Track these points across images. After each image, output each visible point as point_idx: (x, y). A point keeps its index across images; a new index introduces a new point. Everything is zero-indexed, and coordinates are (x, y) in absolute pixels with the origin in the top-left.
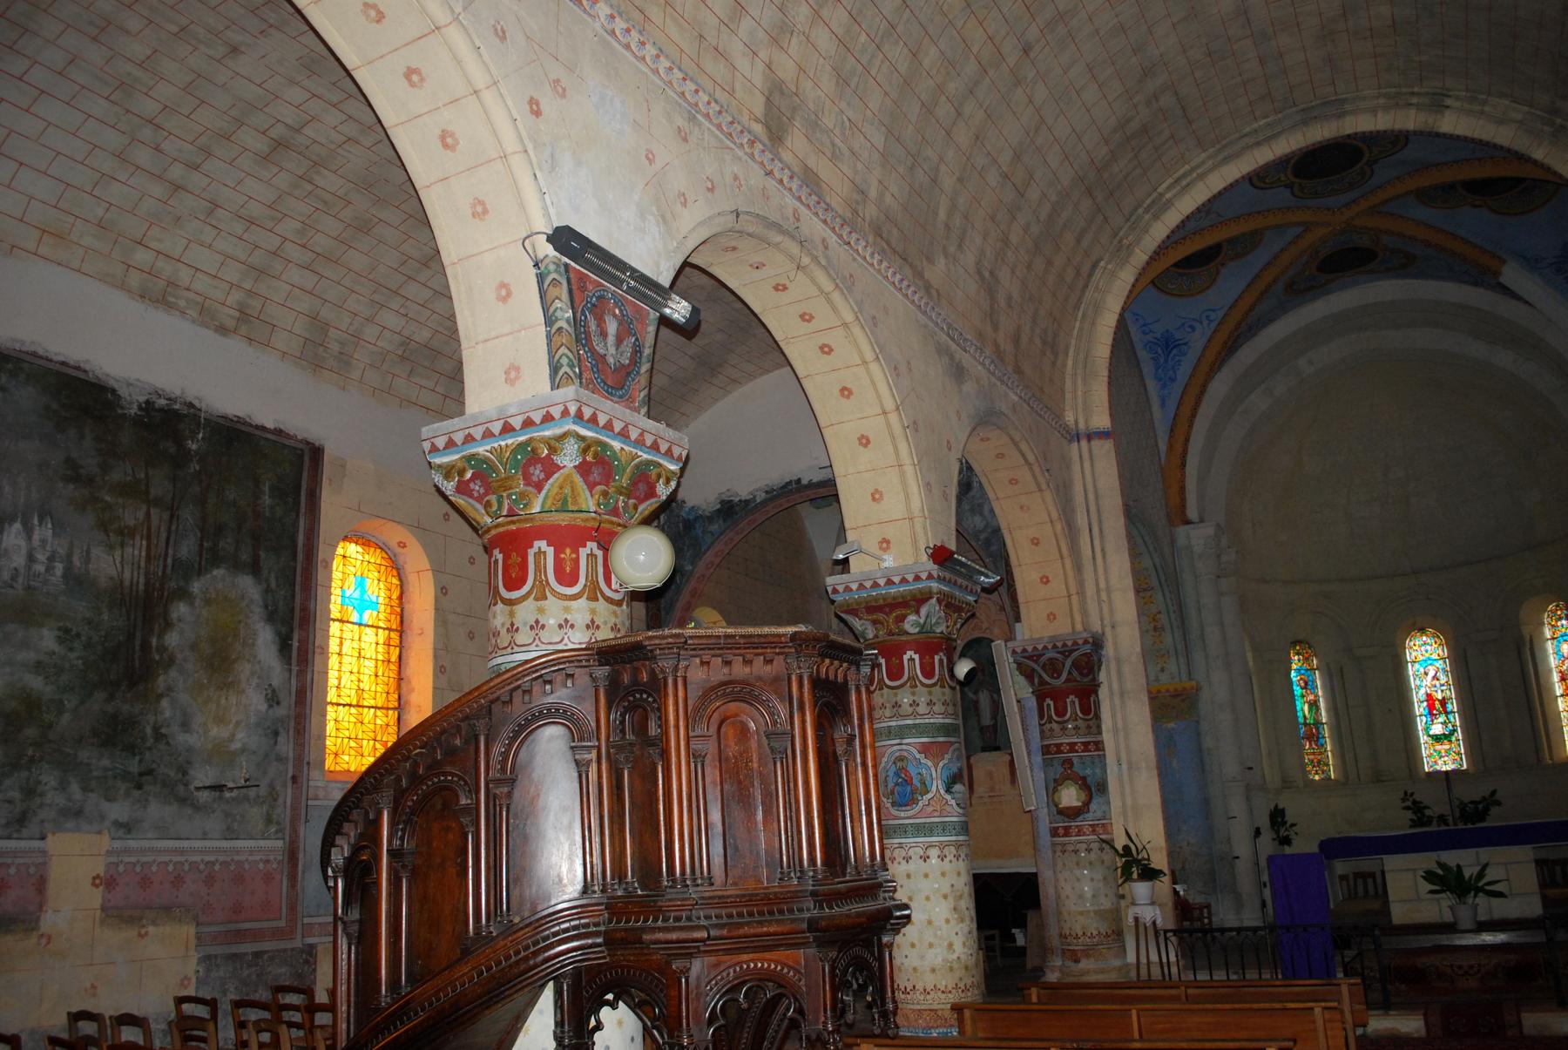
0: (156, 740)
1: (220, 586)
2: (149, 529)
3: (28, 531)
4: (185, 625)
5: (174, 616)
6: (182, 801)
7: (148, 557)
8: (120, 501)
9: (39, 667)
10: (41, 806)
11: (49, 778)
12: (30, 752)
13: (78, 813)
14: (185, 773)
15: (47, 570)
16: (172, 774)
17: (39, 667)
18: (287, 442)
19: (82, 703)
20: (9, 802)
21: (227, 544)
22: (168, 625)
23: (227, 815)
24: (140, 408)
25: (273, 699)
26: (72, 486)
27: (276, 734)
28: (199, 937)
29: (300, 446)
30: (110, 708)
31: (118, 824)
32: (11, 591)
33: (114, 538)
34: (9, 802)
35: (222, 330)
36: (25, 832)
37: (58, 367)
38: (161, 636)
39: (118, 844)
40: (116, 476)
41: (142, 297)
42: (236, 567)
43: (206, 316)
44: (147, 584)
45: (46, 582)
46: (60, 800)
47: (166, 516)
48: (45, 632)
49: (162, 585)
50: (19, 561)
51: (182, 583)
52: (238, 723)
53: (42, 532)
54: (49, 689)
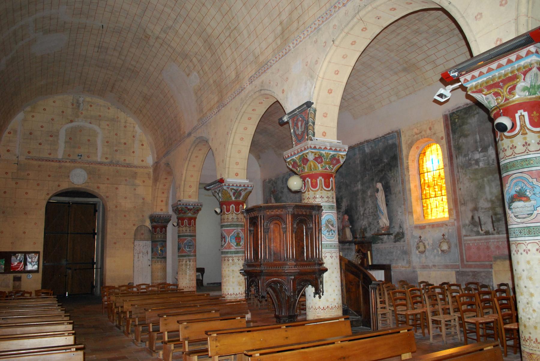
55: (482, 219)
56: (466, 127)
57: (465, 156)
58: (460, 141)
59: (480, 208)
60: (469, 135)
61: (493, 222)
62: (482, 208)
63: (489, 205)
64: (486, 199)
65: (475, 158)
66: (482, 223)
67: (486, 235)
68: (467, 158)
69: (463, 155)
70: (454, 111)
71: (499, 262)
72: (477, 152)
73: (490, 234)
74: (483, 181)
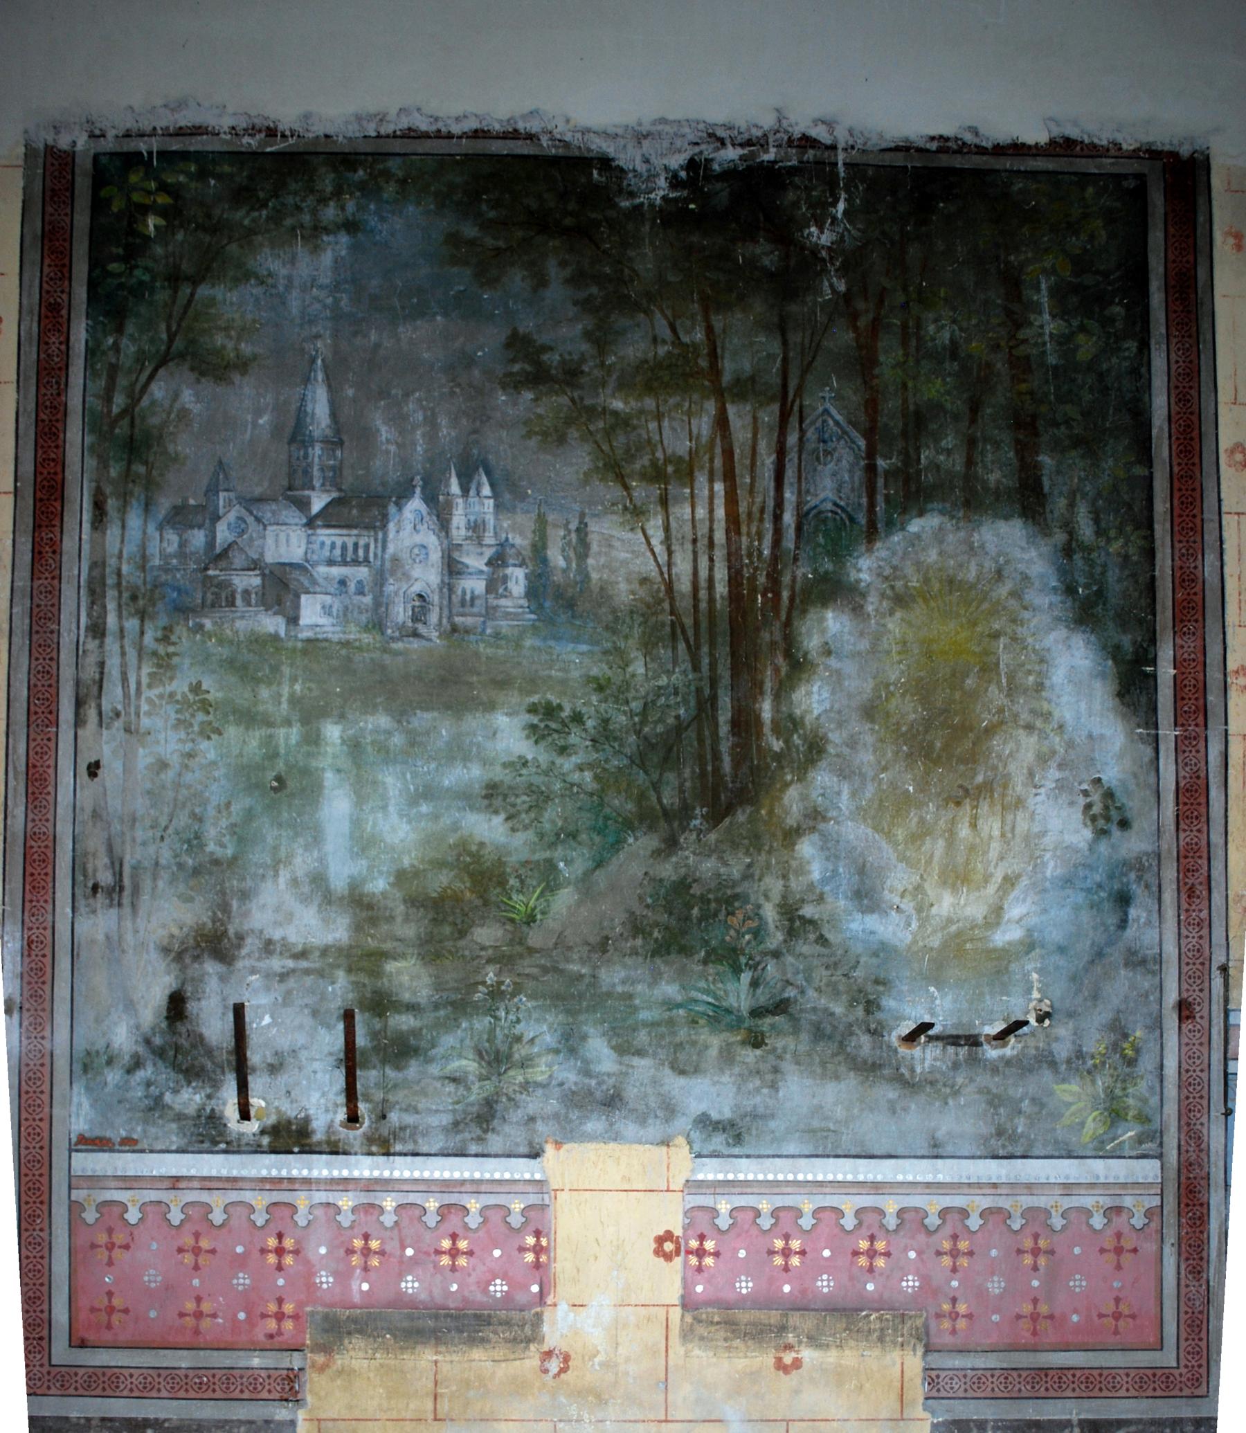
0: (791, 933)
1: (932, 556)
2: (728, 454)
3: (441, 515)
4: (843, 667)
5: (811, 643)
6: (869, 1069)
7: (733, 521)
8: (649, 403)
10: (526, 1086)
11: (538, 1028)
12: (491, 977)
13: (612, 1102)
14: (871, 1006)
15: (491, 588)
16: (838, 1009)
18: (1091, 167)
21: (942, 453)
22: (798, 667)
23: (994, 1101)
25: (1108, 814)
26: (528, 395)
27: (1123, 900)
28: (932, 1377)
29: (1134, 167)
30: (667, 870)
31: (706, 1124)
32: (415, 644)
33: (641, 491)
34: (454, 1080)
36: (495, 1142)
37: (466, 146)
38: (783, 690)
39: (711, 1171)
40: (634, 348)
42: (972, 501)
44: (734, 579)
45: (490, 612)
46: (569, 1075)
47: (769, 415)
48: (501, 720)
50: (427, 577)
51: (828, 566)
52: (1010, 882)
53: (474, 507)
54: (520, 839)
55: (260, 1023)
56: (229, 301)
57: (180, 517)
58: (158, 390)
59: (251, 944)
60: (243, 365)
61: (351, 1061)
62: (268, 947)
63: (338, 931)
64: (318, 880)
65: (269, 558)
66: (255, 1057)
67: (274, 1151)
68: (198, 538)
69: (164, 504)
70: (143, 146)
71: (356, 1356)
72: (293, 516)
73: (308, 1149)
74: (313, 739)
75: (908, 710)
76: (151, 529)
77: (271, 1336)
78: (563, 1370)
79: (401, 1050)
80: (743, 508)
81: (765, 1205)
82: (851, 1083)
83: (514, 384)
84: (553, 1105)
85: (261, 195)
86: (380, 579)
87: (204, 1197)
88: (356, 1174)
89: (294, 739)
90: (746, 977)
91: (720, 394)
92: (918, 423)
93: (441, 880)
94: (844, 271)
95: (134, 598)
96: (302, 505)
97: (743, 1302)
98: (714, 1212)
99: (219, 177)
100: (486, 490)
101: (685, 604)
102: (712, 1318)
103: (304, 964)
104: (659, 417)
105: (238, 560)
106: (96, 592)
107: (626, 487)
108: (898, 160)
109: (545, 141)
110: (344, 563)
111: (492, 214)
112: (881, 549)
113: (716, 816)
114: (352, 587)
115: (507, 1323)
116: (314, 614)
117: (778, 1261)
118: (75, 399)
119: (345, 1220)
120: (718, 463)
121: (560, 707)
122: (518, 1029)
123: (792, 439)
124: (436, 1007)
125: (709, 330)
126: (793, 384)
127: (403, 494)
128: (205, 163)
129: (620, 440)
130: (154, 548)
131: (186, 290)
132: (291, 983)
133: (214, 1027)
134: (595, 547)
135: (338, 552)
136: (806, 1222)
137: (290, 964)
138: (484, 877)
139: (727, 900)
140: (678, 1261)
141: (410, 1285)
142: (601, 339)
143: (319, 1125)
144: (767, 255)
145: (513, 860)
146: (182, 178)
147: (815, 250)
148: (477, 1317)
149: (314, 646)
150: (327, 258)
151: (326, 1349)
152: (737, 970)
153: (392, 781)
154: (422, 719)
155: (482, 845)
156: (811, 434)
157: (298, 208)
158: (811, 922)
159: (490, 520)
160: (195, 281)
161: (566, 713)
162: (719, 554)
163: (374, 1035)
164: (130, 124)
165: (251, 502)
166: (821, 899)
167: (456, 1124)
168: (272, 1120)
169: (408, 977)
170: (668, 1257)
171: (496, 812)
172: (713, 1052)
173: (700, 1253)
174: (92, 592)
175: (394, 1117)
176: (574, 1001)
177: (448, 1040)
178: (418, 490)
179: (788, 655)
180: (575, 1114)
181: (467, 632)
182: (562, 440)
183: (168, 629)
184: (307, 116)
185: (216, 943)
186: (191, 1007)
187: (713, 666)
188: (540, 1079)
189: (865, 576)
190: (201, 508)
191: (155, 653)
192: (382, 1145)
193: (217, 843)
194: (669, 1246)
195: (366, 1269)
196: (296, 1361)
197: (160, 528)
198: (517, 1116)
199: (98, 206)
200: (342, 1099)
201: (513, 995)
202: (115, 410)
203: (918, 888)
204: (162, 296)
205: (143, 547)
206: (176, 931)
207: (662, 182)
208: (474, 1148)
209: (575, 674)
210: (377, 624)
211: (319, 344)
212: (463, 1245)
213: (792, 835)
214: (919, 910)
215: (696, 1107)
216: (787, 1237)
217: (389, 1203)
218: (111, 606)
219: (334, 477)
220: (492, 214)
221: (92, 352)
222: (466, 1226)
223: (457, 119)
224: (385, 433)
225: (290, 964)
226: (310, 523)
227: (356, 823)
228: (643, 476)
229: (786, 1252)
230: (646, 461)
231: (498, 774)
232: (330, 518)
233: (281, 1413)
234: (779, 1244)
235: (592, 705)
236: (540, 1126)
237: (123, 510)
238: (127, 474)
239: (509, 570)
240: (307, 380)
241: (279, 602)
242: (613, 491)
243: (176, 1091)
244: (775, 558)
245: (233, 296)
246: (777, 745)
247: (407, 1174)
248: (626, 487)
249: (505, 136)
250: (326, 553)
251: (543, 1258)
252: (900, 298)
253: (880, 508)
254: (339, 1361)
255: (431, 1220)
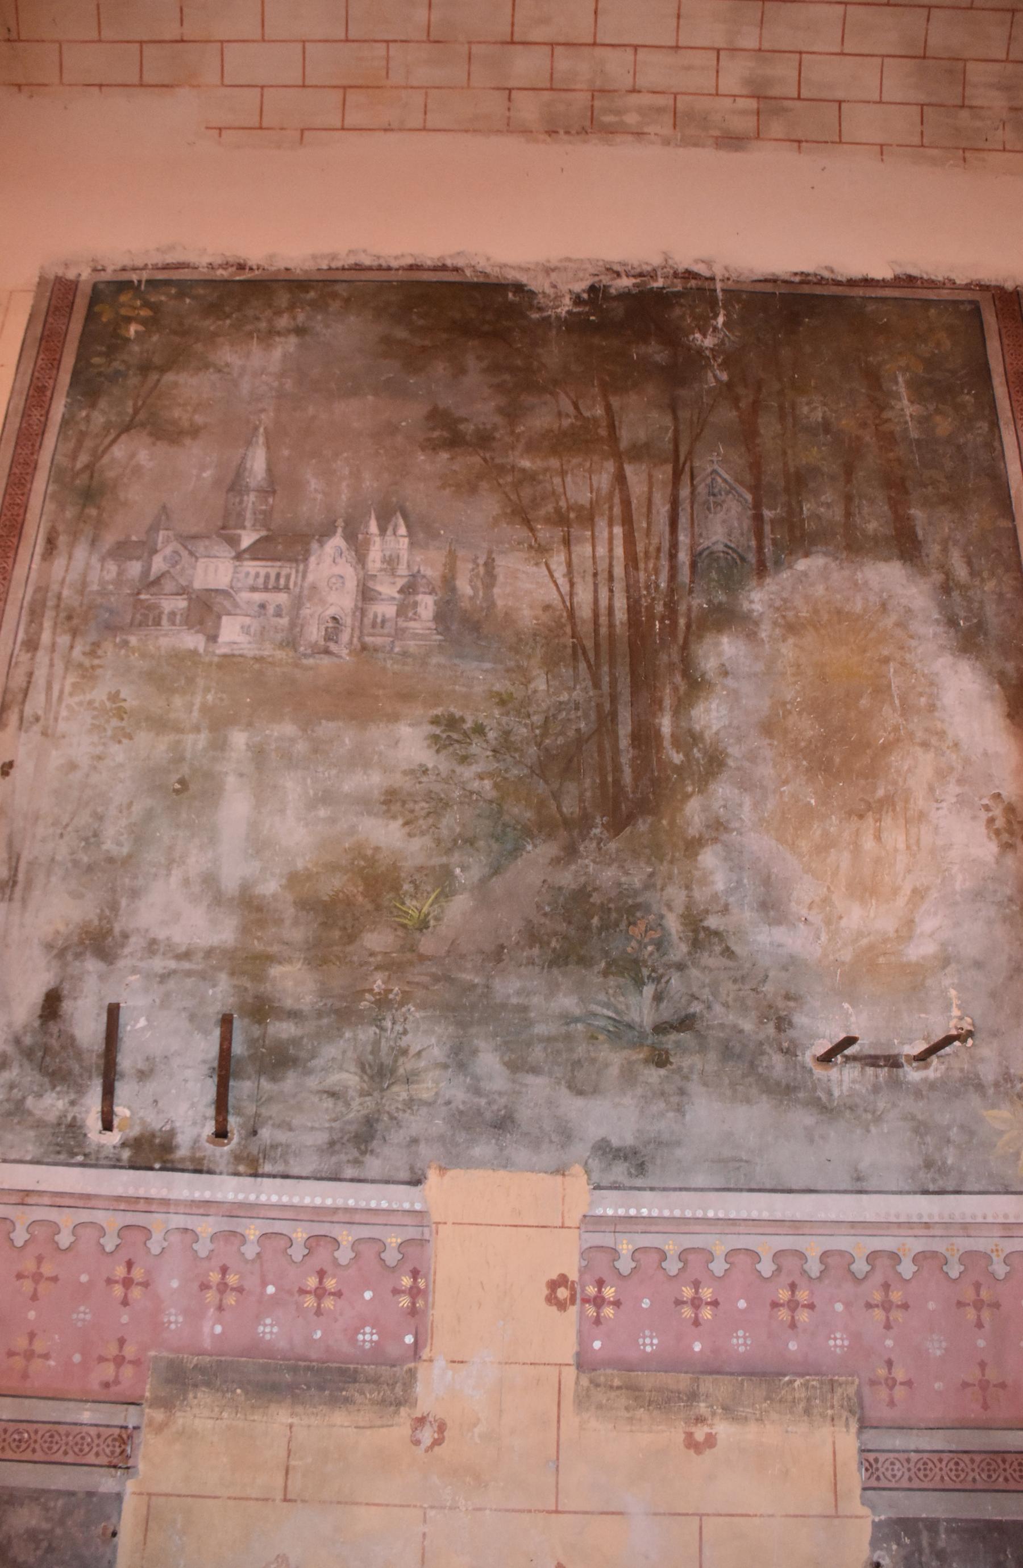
0: (696, 945)
1: (820, 590)
2: (626, 503)
3: (359, 550)
4: (737, 687)
6: (784, 1092)
7: (632, 560)
8: (554, 463)
9: (391, 801)
10: (410, 1103)
11: (425, 1040)
12: (378, 983)
13: (503, 1123)
14: (783, 1023)
16: (747, 1026)
17: (391, 801)
18: (932, 295)
19: (496, 870)
20: (333, 1094)
21: (822, 505)
22: (696, 685)
23: (921, 1128)
24: (577, 300)
26: (445, 455)
28: (869, 1461)
29: (968, 296)
30: (567, 878)
31: (607, 1151)
32: (326, 661)
33: (544, 532)
34: (333, 1094)
35: (732, 141)
36: (374, 1166)
37: (402, 276)
38: (683, 706)
41: (552, 132)
42: (854, 546)
43: (687, 124)
44: (633, 609)
45: (399, 633)
47: (664, 473)
48: (404, 730)
49: (671, 608)
50: (341, 602)
51: (721, 597)
52: (918, 894)
53: (390, 545)
54: (417, 844)
57: (122, 551)
58: (119, 451)
59: (135, 943)
60: (195, 432)
61: (225, 1070)
62: (152, 947)
63: (224, 932)
64: (210, 880)
65: (197, 585)
66: (126, 1062)
67: (133, 1167)
68: (135, 568)
69: (109, 539)
70: (135, 277)
71: (202, 1415)
73: (169, 1167)
74: (219, 745)
75: (806, 728)
76: (95, 561)
77: (107, 1385)
78: (437, 1442)
79: (278, 1060)
80: (640, 548)
81: (671, 1246)
82: (763, 1107)
83: (433, 446)
84: (439, 1125)
85: (227, 309)
86: (298, 603)
87: (53, 1215)
88: (219, 1197)
89: (200, 746)
90: (649, 990)
91: (618, 456)
92: (799, 482)
93: (336, 883)
94: (725, 365)
95: (69, 618)
96: (233, 541)
97: (645, 1364)
98: (614, 1253)
99: (193, 297)
100: (402, 530)
101: (586, 630)
102: (615, 1381)
103: (186, 965)
104: (563, 473)
105: (169, 586)
106: (35, 613)
107: (532, 530)
108: (769, 288)
109: (468, 272)
110: (266, 589)
111: (421, 322)
112: (771, 584)
113: (617, 825)
114: (271, 610)
115: (375, 1381)
116: (233, 633)
117: (687, 1312)
118: (45, 458)
119: (203, 1248)
120: (617, 510)
121: (463, 720)
122: (403, 1042)
123: (685, 492)
124: (320, 1014)
125: (608, 408)
126: (683, 450)
127: (326, 532)
128: (184, 288)
129: (527, 492)
130: (94, 577)
131: (154, 376)
132: (171, 984)
133: (86, 1027)
134: (501, 578)
135: (261, 580)
136: (718, 1267)
137: (173, 964)
138: (379, 881)
139: (627, 910)
140: (573, 1310)
141: (269, 1330)
142: (512, 414)
143: (184, 1141)
144: (657, 353)
145: (408, 865)
146: (163, 298)
147: (700, 351)
148: (342, 1372)
149: (230, 662)
150: (277, 353)
151: (166, 1404)
152: (639, 983)
153: (293, 786)
154: (326, 728)
155: (377, 849)
156: (701, 489)
157: (258, 319)
158: (716, 933)
159: (404, 555)
160: (163, 370)
161: (468, 725)
162: (619, 586)
163: (252, 1043)
164: (127, 261)
165: (188, 539)
166: (725, 910)
167: (332, 1144)
168: (135, 1132)
169: (293, 982)
170: (562, 1306)
171: (394, 817)
172: (614, 1071)
173: (599, 1302)
174: (32, 612)
175: (266, 1133)
176: (466, 1011)
177: (330, 1051)
178: (340, 530)
179: (686, 674)
180: (461, 1137)
181: (376, 650)
182: (473, 489)
183: (96, 645)
184: (272, 256)
185: (99, 942)
186: (67, 1006)
187: (613, 683)
188: (425, 1096)
189: (758, 607)
190: (142, 543)
191: (80, 665)
192: (251, 1165)
193: (114, 840)
194: (562, 1293)
195: (220, 1308)
196: (131, 1417)
197: (103, 560)
198: (398, 1137)
199: (91, 316)
200: (211, 1112)
201: (402, 1004)
202: (79, 465)
203: (826, 901)
204: (133, 381)
205: (84, 575)
206: (62, 928)
207: (567, 301)
208: (349, 1172)
209: (478, 689)
210: (291, 643)
211: (263, 416)
212: (330, 1284)
213: (693, 846)
214: (828, 922)
215: (594, 1132)
216: (696, 1285)
217: (253, 1231)
218: (47, 624)
219: (264, 519)
220: (421, 322)
221: (66, 422)
222: (335, 1262)
223: (396, 258)
224: (314, 484)
225: (173, 964)
226: (239, 557)
227: (254, 826)
228: (547, 520)
229: (696, 1303)
230: (550, 508)
231: (398, 780)
232: (257, 552)
233: (107, 1483)
234: (688, 1292)
235: (493, 719)
236: (423, 1149)
237: (72, 545)
238: (81, 517)
239: (419, 598)
240: (249, 443)
241: (201, 622)
242: (521, 532)
243: (39, 1096)
244: (671, 590)
245: (194, 381)
246: (677, 758)
247: (274, 1199)
248: (532, 530)
249: (435, 269)
250: (250, 581)
251: (421, 1283)
252: (776, 386)
253: (768, 550)
254: (182, 1419)
255: (298, 1252)
